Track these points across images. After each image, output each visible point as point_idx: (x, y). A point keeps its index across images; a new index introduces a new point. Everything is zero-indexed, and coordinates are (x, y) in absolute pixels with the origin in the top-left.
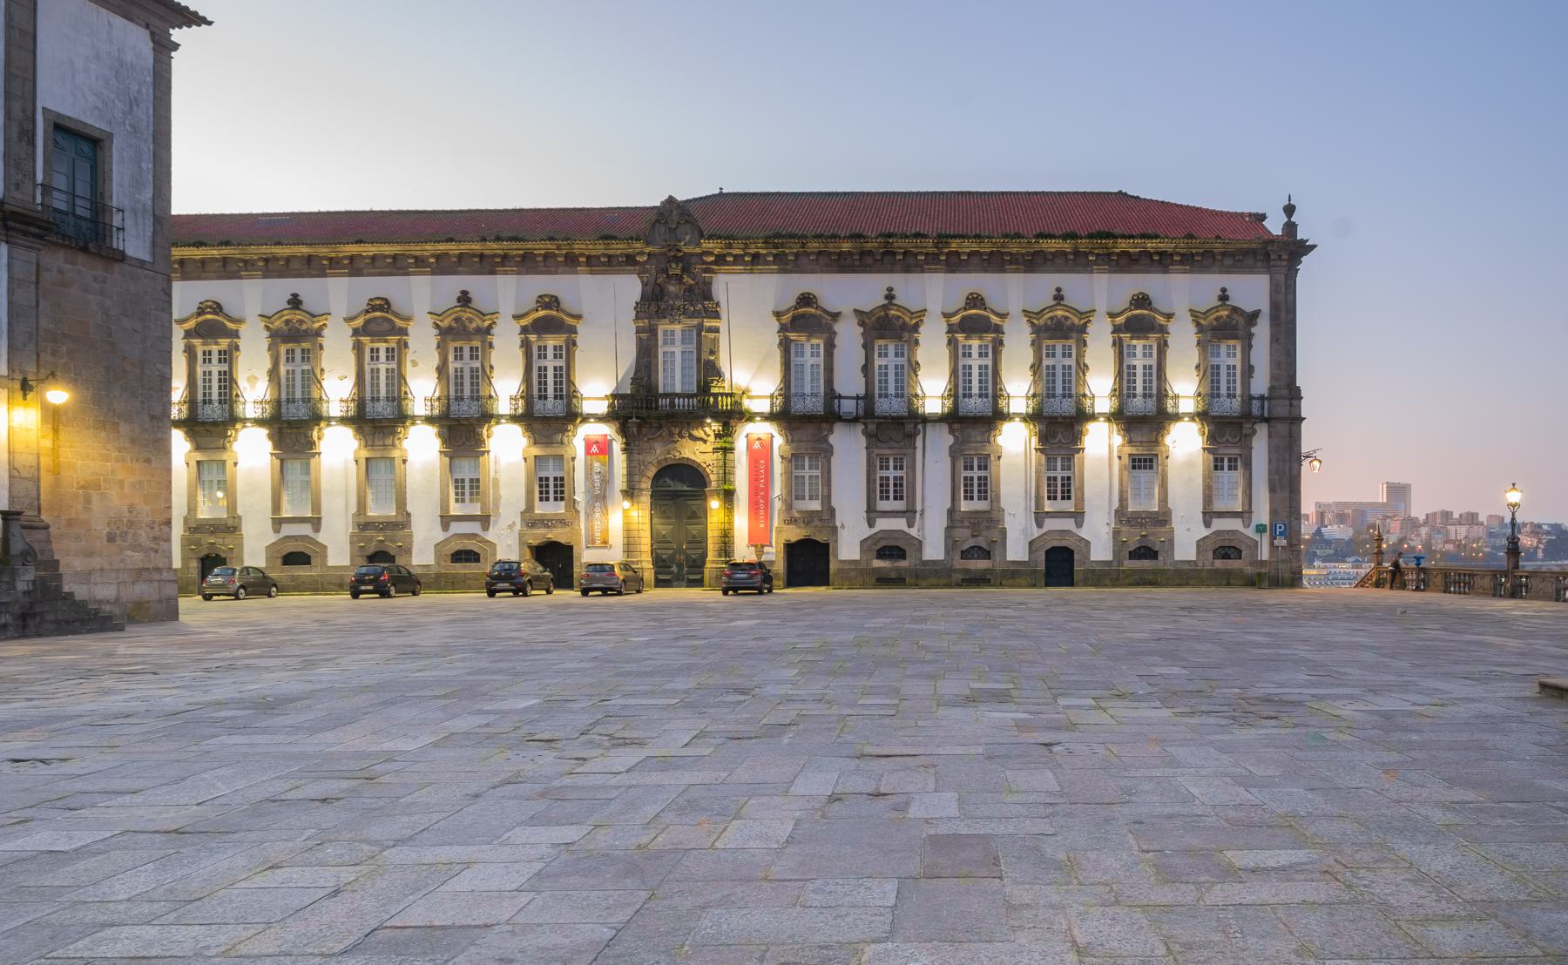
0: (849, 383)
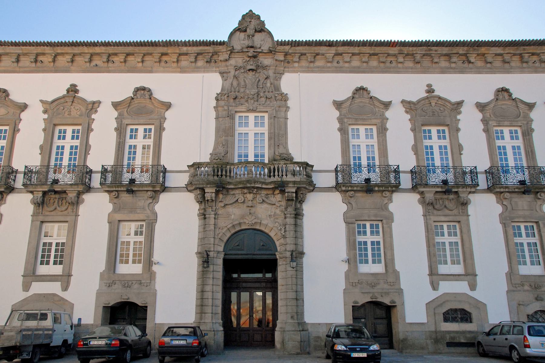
0: (402, 157)
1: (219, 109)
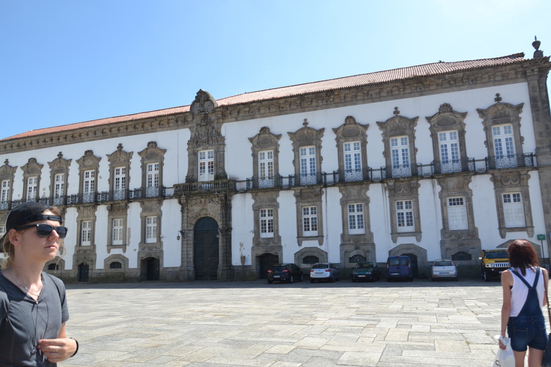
0: (286, 169)
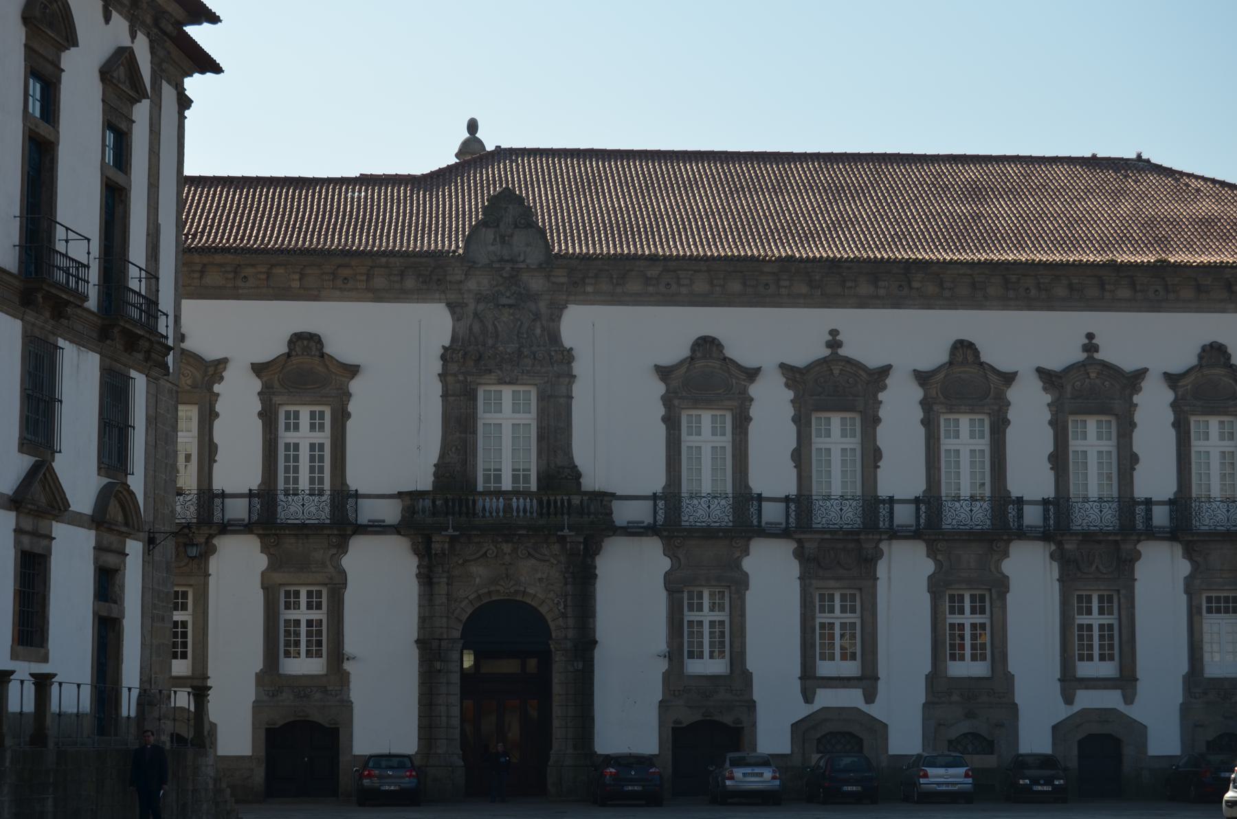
1: (450, 379)
